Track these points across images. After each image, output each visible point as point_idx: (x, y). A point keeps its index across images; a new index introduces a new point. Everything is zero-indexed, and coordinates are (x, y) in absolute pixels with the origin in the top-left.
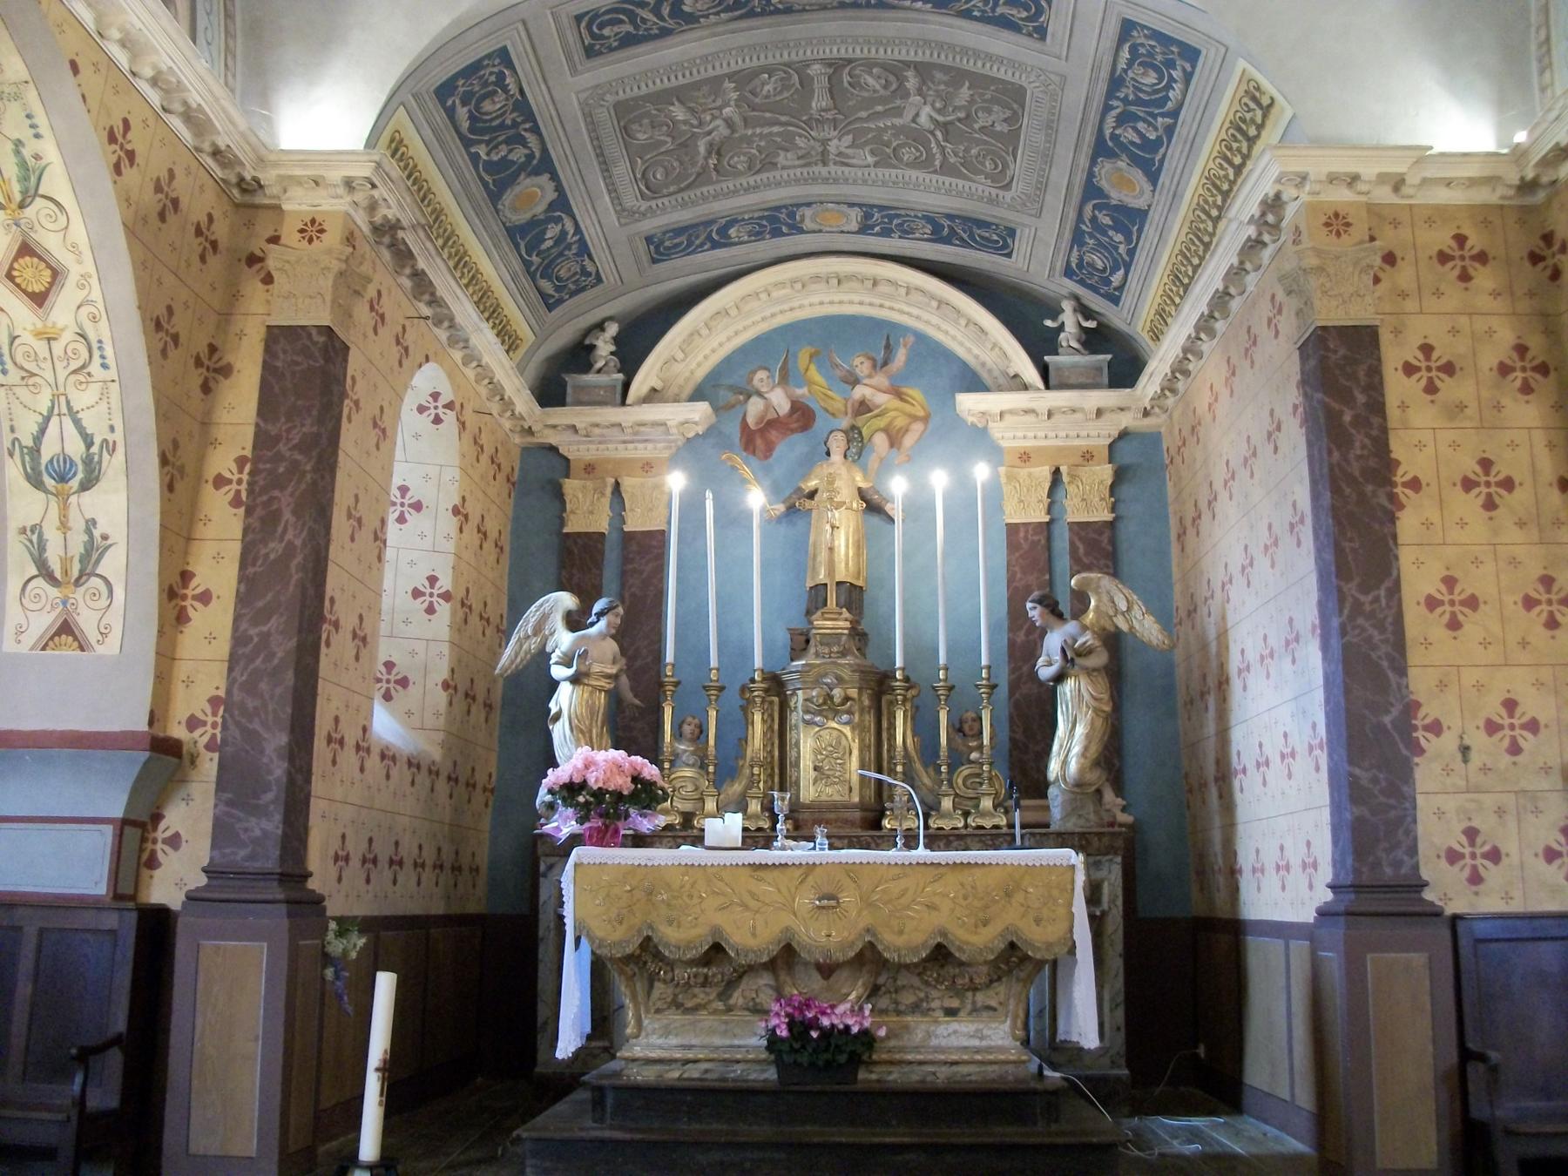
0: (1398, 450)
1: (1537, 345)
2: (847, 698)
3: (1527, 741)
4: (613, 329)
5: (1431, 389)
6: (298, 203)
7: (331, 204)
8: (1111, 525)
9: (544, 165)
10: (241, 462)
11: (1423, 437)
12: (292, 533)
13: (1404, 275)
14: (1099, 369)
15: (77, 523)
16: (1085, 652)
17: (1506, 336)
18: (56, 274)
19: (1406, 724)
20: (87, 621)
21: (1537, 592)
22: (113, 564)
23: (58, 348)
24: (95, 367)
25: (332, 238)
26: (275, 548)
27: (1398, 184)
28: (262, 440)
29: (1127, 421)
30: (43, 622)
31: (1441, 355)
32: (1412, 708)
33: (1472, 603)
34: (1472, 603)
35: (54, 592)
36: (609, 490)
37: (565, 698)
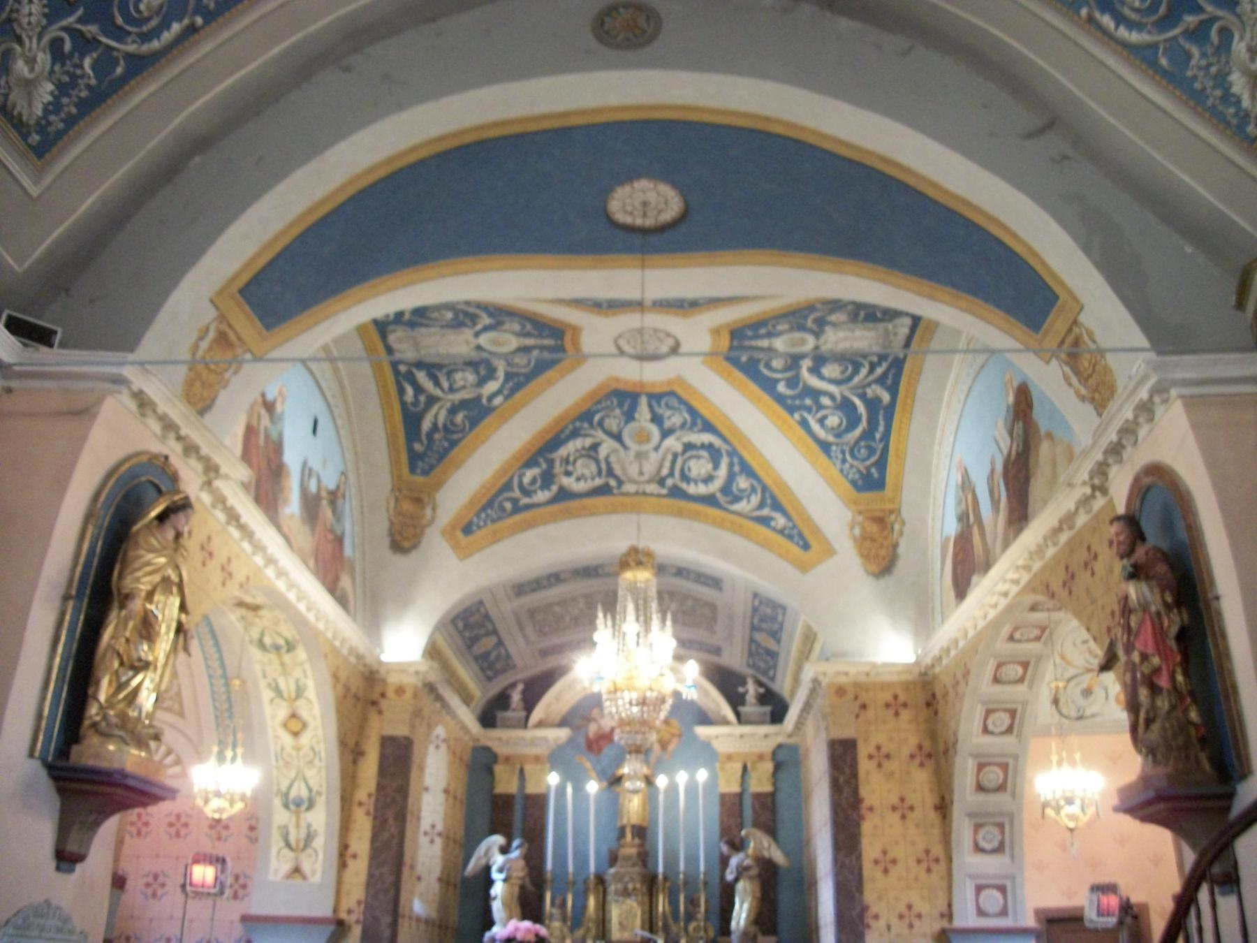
0: (864, 792)
1: (927, 744)
2: (635, 889)
3: (916, 923)
4: (520, 687)
5: (880, 765)
6: (394, 679)
7: (410, 680)
8: (773, 795)
9: (495, 632)
10: (370, 796)
11: (875, 788)
12: (392, 828)
13: (870, 714)
14: (765, 714)
15: (303, 824)
16: (747, 868)
17: (913, 741)
18: (305, 725)
19: (861, 916)
20: (306, 867)
21: (923, 856)
22: (318, 843)
23: (301, 753)
24: (317, 762)
25: (409, 694)
26: (386, 835)
27: (868, 674)
28: (380, 787)
29: (781, 739)
30: (286, 867)
31: (884, 750)
32: (865, 908)
33: (894, 862)
34: (894, 862)
35: (291, 855)
36: (517, 771)
37: (498, 889)
